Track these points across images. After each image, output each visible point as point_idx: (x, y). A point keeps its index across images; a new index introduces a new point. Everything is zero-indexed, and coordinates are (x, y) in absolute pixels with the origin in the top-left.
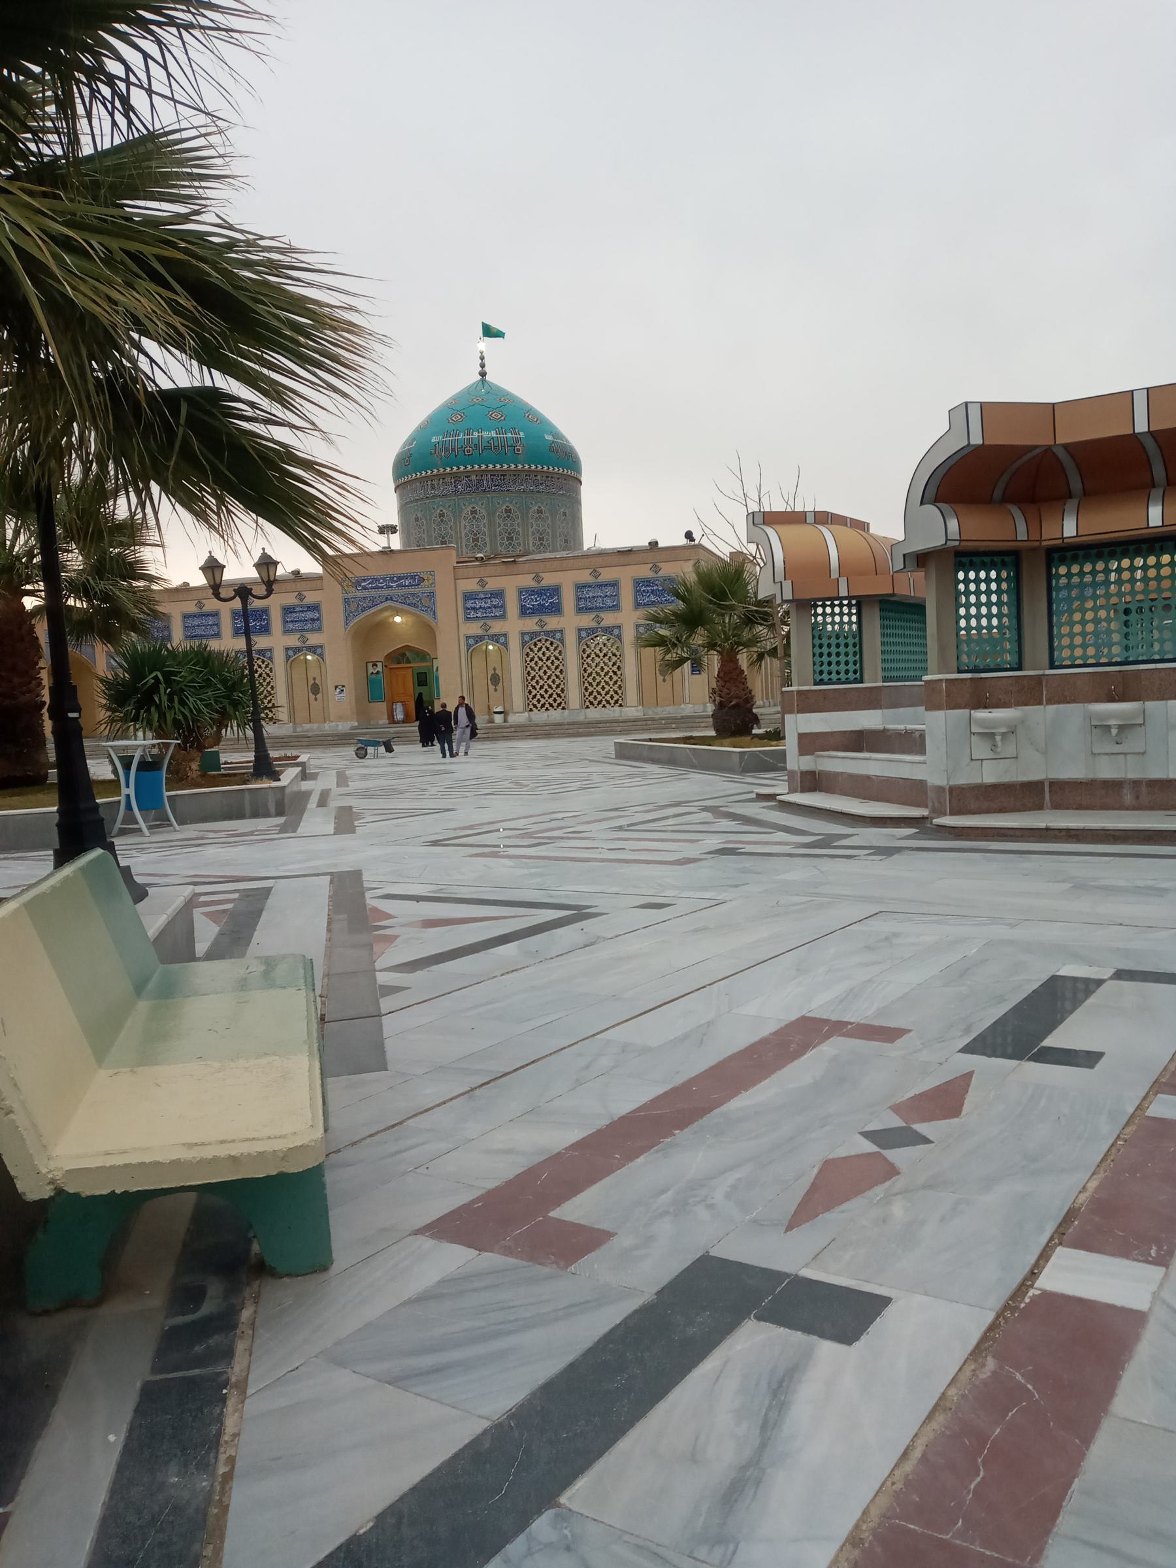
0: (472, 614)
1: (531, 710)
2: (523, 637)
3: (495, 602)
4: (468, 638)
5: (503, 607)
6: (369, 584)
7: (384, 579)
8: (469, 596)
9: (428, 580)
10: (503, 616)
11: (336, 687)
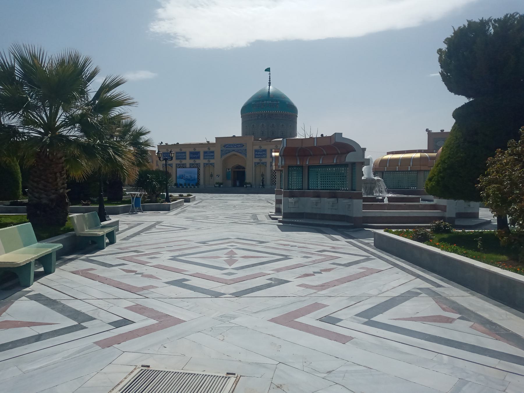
0: (257, 156)
1: (272, 185)
2: (265, 163)
3: (264, 153)
4: (255, 163)
5: (266, 154)
7: (233, 145)
8: (256, 151)
10: (266, 157)
11: (217, 175)
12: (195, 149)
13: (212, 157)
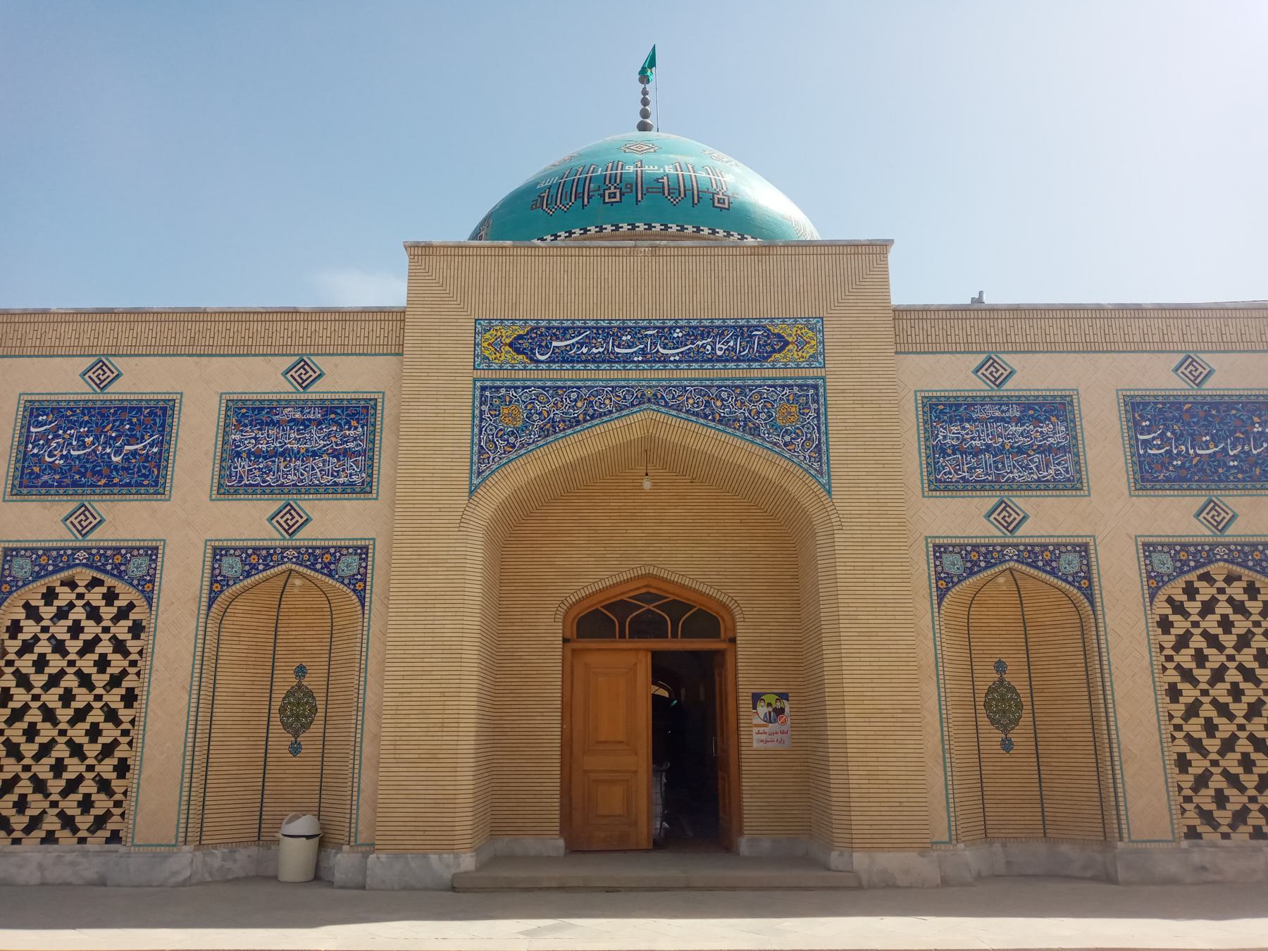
4: (939, 550)
6: (582, 344)
7: (636, 331)
9: (801, 343)
10: (1073, 483)
12: (101, 372)
13: (352, 471)
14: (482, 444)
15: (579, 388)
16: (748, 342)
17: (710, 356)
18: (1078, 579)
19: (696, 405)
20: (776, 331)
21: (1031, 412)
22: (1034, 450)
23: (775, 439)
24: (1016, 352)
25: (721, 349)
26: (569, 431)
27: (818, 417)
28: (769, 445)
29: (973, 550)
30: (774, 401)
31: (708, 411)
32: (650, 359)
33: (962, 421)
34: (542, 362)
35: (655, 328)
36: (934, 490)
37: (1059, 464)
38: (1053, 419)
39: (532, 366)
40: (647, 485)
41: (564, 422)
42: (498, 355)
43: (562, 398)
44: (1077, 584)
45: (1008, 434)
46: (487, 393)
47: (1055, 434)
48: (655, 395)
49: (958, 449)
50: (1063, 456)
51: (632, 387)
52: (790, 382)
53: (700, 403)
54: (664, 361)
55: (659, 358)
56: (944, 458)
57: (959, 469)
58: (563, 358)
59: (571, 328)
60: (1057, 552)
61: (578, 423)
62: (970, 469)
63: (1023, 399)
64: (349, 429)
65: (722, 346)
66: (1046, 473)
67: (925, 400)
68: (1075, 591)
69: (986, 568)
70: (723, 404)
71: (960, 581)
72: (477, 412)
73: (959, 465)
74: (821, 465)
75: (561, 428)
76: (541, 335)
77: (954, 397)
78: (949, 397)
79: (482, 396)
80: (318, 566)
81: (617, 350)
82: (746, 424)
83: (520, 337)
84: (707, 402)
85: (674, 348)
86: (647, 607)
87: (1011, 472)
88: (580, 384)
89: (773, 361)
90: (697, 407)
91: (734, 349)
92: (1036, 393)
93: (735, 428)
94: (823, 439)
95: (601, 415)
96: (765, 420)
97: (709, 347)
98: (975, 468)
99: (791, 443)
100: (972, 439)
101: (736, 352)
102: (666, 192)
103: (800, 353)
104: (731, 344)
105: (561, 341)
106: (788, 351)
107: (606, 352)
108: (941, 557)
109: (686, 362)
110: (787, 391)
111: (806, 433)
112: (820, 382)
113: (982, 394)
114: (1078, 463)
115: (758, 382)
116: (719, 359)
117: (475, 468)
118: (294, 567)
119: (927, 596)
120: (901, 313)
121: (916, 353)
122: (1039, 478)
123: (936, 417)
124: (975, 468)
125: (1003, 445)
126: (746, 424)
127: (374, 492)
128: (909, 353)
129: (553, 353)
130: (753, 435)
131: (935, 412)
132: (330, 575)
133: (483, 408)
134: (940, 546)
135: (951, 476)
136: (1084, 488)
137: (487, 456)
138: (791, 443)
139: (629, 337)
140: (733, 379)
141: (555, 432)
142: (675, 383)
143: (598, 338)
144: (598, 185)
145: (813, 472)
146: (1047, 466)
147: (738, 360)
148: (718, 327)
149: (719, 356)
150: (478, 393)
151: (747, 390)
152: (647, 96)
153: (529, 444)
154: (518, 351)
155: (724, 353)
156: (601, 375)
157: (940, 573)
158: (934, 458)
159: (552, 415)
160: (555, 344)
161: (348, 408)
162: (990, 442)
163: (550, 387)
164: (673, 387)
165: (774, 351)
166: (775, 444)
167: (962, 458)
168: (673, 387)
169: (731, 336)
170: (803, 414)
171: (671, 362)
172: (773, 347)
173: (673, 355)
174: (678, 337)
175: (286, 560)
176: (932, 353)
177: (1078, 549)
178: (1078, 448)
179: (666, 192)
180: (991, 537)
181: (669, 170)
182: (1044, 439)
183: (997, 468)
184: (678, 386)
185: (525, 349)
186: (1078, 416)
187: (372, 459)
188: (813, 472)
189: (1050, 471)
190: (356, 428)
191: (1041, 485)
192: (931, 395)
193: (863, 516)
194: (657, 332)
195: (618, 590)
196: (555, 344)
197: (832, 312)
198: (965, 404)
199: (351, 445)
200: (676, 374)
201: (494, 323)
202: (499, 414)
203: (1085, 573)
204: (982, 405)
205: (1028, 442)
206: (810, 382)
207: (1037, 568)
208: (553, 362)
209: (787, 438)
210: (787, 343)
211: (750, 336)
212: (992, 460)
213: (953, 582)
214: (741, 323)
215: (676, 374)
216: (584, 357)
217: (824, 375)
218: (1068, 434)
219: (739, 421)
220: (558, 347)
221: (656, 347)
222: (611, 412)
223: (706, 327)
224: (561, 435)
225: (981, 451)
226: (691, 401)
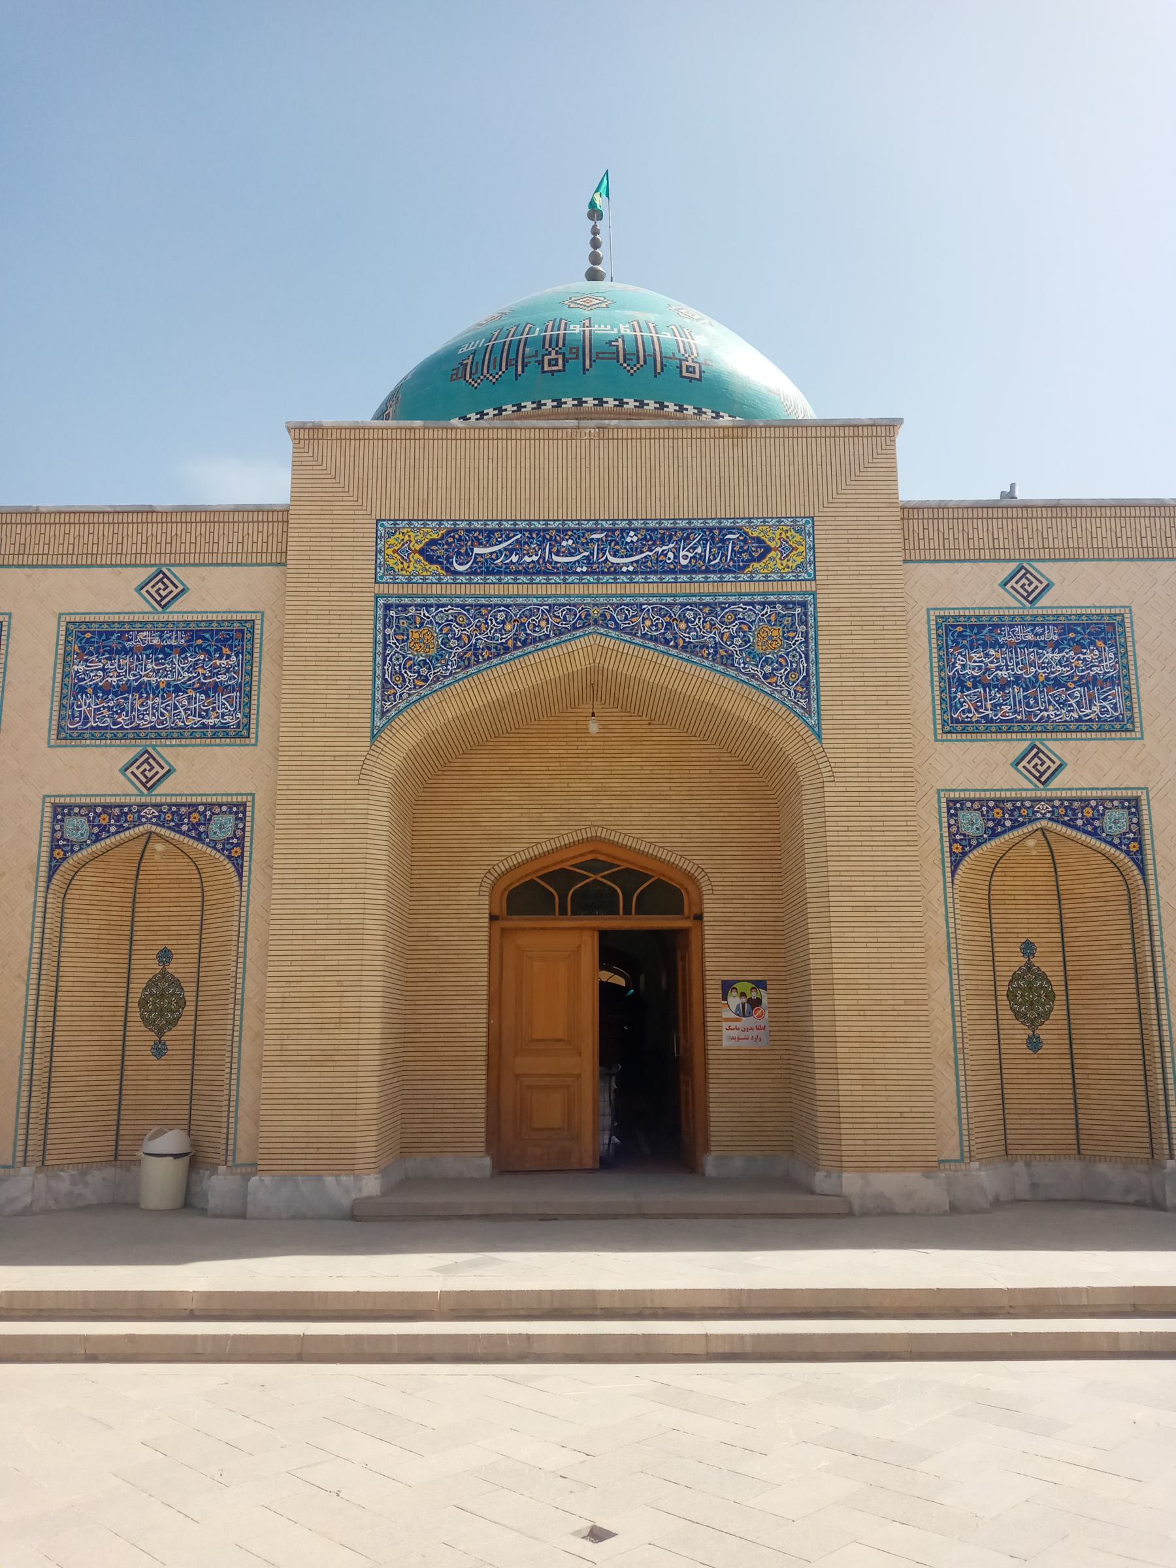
4: (955, 806)
5: (1121, 679)
6: (510, 551)
7: (580, 535)
9: (787, 550)
13: (225, 711)
14: (386, 676)
15: (507, 606)
16: (720, 548)
17: (672, 566)
18: (1126, 841)
19: (654, 628)
20: (755, 534)
21: (1072, 635)
22: (1074, 682)
23: (752, 669)
24: (1055, 560)
25: (686, 557)
26: (495, 661)
27: (806, 642)
28: (744, 678)
29: (996, 806)
30: (751, 623)
31: (669, 635)
32: (597, 570)
33: (985, 646)
34: (461, 573)
35: (603, 530)
36: (950, 732)
37: (1105, 699)
38: (1100, 644)
39: (448, 579)
40: (594, 727)
41: (489, 649)
42: (406, 565)
43: (486, 620)
44: (1124, 848)
45: (1043, 663)
46: (393, 613)
47: (1101, 661)
48: (603, 615)
49: (980, 682)
50: (1110, 690)
51: (574, 605)
52: (772, 598)
53: (660, 626)
54: (615, 572)
55: (609, 569)
56: (962, 692)
57: (981, 706)
58: (487, 568)
59: (497, 530)
60: (1101, 808)
61: (507, 650)
62: (994, 705)
63: (1062, 618)
64: (220, 658)
65: (688, 553)
66: (1088, 711)
67: (940, 621)
68: (1123, 856)
69: (1012, 828)
70: (688, 626)
71: (979, 844)
72: (380, 637)
73: (980, 701)
74: (809, 702)
75: (486, 657)
76: (460, 539)
77: (976, 616)
78: (970, 617)
79: (385, 616)
80: (185, 828)
81: (555, 558)
82: (716, 652)
83: (433, 542)
84: (668, 623)
85: (627, 556)
86: (593, 877)
87: (1046, 710)
88: (508, 601)
89: (751, 572)
90: (656, 631)
91: (702, 557)
92: (1079, 612)
93: (702, 657)
94: (813, 669)
95: (535, 640)
96: (740, 646)
97: (670, 555)
98: (1001, 705)
99: (772, 674)
100: (998, 668)
101: (704, 562)
102: (621, 361)
103: (785, 562)
104: (699, 550)
105: (485, 547)
106: (770, 559)
107: (541, 561)
108: (956, 815)
109: (642, 573)
110: (768, 609)
111: (791, 662)
112: (810, 598)
113: (1011, 613)
114: (1129, 698)
115: (732, 599)
116: (684, 570)
117: (378, 706)
118: (154, 828)
119: (938, 862)
120: (911, 511)
121: (930, 561)
122: (1079, 716)
123: (953, 642)
124: (1001, 705)
125: (1036, 676)
126: (716, 652)
127: (251, 736)
128: (920, 561)
129: (475, 562)
130: (725, 665)
131: (952, 635)
132: (199, 839)
133: (388, 631)
134: (955, 802)
135: (970, 715)
136: (1136, 730)
137: (393, 691)
138: (772, 674)
139: (570, 542)
140: (700, 595)
141: (478, 662)
142: (627, 600)
143: (532, 543)
144: (534, 349)
145: (798, 710)
146: (1090, 701)
147: (707, 571)
148: (683, 529)
149: (683, 566)
150: (380, 612)
151: (718, 609)
152: (598, 236)
153: (445, 677)
154: (431, 560)
155: (690, 562)
156: (536, 590)
157: (955, 835)
158: (950, 693)
159: (474, 641)
160: (477, 550)
161: (218, 631)
162: (1020, 672)
163: (471, 605)
164: (625, 605)
165: (753, 560)
166: (753, 676)
167: (985, 691)
168: (625, 605)
169: (699, 541)
170: (788, 638)
171: (623, 573)
172: (750, 554)
173: (626, 565)
174: (632, 542)
175: (144, 820)
176: (950, 561)
177: (1126, 804)
178: (1129, 680)
179: (621, 358)
180: (1019, 790)
181: (626, 330)
182: (1088, 669)
183: (1028, 705)
184: (632, 604)
185: (440, 557)
186: (1130, 639)
187: (249, 695)
188: (798, 710)
189: (1094, 708)
190: (229, 657)
191: (1083, 725)
192: (947, 613)
193: (860, 765)
194: (606, 536)
195: (557, 857)
196: (477, 550)
197: (825, 510)
198: (990, 625)
199: (223, 678)
200: (630, 589)
201: (401, 524)
202: (408, 639)
203: (1135, 833)
204: (1011, 626)
205: (1067, 672)
206: (798, 598)
207: (1075, 827)
208: (475, 573)
209: (768, 669)
210: (768, 549)
211: (723, 541)
212: (1022, 694)
213: (970, 845)
214: (712, 524)
215: (630, 589)
216: (513, 568)
217: (814, 589)
218: (1117, 662)
219: (708, 648)
220: (481, 555)
221: (604, 554)
222: (547, 637)
223: (668, 529)
224: (485, 665)
225: (1008, 684)
226: (648, 623)
